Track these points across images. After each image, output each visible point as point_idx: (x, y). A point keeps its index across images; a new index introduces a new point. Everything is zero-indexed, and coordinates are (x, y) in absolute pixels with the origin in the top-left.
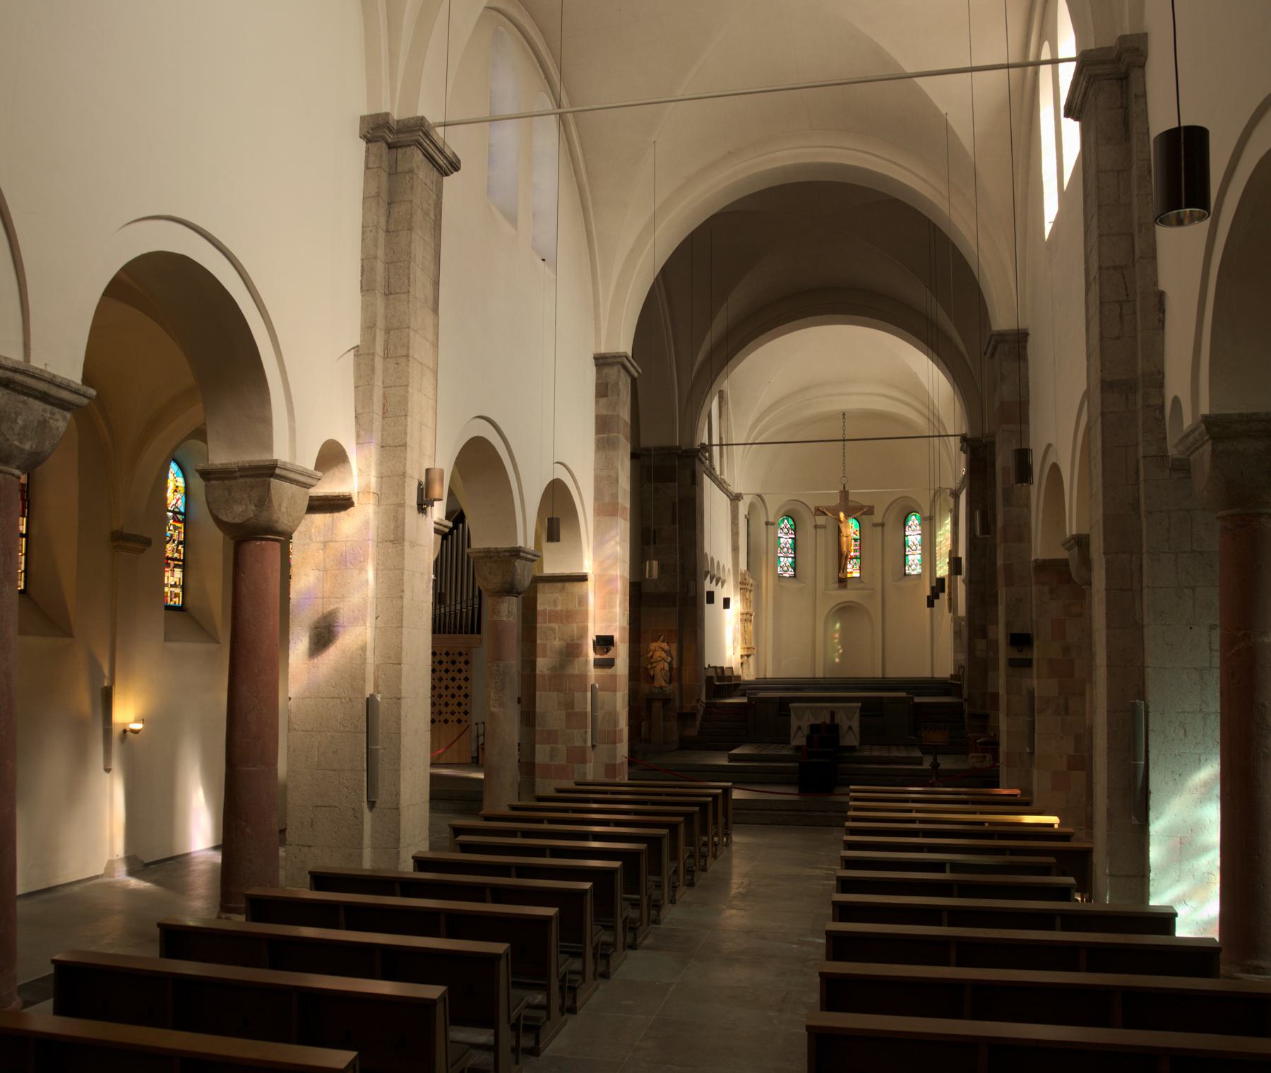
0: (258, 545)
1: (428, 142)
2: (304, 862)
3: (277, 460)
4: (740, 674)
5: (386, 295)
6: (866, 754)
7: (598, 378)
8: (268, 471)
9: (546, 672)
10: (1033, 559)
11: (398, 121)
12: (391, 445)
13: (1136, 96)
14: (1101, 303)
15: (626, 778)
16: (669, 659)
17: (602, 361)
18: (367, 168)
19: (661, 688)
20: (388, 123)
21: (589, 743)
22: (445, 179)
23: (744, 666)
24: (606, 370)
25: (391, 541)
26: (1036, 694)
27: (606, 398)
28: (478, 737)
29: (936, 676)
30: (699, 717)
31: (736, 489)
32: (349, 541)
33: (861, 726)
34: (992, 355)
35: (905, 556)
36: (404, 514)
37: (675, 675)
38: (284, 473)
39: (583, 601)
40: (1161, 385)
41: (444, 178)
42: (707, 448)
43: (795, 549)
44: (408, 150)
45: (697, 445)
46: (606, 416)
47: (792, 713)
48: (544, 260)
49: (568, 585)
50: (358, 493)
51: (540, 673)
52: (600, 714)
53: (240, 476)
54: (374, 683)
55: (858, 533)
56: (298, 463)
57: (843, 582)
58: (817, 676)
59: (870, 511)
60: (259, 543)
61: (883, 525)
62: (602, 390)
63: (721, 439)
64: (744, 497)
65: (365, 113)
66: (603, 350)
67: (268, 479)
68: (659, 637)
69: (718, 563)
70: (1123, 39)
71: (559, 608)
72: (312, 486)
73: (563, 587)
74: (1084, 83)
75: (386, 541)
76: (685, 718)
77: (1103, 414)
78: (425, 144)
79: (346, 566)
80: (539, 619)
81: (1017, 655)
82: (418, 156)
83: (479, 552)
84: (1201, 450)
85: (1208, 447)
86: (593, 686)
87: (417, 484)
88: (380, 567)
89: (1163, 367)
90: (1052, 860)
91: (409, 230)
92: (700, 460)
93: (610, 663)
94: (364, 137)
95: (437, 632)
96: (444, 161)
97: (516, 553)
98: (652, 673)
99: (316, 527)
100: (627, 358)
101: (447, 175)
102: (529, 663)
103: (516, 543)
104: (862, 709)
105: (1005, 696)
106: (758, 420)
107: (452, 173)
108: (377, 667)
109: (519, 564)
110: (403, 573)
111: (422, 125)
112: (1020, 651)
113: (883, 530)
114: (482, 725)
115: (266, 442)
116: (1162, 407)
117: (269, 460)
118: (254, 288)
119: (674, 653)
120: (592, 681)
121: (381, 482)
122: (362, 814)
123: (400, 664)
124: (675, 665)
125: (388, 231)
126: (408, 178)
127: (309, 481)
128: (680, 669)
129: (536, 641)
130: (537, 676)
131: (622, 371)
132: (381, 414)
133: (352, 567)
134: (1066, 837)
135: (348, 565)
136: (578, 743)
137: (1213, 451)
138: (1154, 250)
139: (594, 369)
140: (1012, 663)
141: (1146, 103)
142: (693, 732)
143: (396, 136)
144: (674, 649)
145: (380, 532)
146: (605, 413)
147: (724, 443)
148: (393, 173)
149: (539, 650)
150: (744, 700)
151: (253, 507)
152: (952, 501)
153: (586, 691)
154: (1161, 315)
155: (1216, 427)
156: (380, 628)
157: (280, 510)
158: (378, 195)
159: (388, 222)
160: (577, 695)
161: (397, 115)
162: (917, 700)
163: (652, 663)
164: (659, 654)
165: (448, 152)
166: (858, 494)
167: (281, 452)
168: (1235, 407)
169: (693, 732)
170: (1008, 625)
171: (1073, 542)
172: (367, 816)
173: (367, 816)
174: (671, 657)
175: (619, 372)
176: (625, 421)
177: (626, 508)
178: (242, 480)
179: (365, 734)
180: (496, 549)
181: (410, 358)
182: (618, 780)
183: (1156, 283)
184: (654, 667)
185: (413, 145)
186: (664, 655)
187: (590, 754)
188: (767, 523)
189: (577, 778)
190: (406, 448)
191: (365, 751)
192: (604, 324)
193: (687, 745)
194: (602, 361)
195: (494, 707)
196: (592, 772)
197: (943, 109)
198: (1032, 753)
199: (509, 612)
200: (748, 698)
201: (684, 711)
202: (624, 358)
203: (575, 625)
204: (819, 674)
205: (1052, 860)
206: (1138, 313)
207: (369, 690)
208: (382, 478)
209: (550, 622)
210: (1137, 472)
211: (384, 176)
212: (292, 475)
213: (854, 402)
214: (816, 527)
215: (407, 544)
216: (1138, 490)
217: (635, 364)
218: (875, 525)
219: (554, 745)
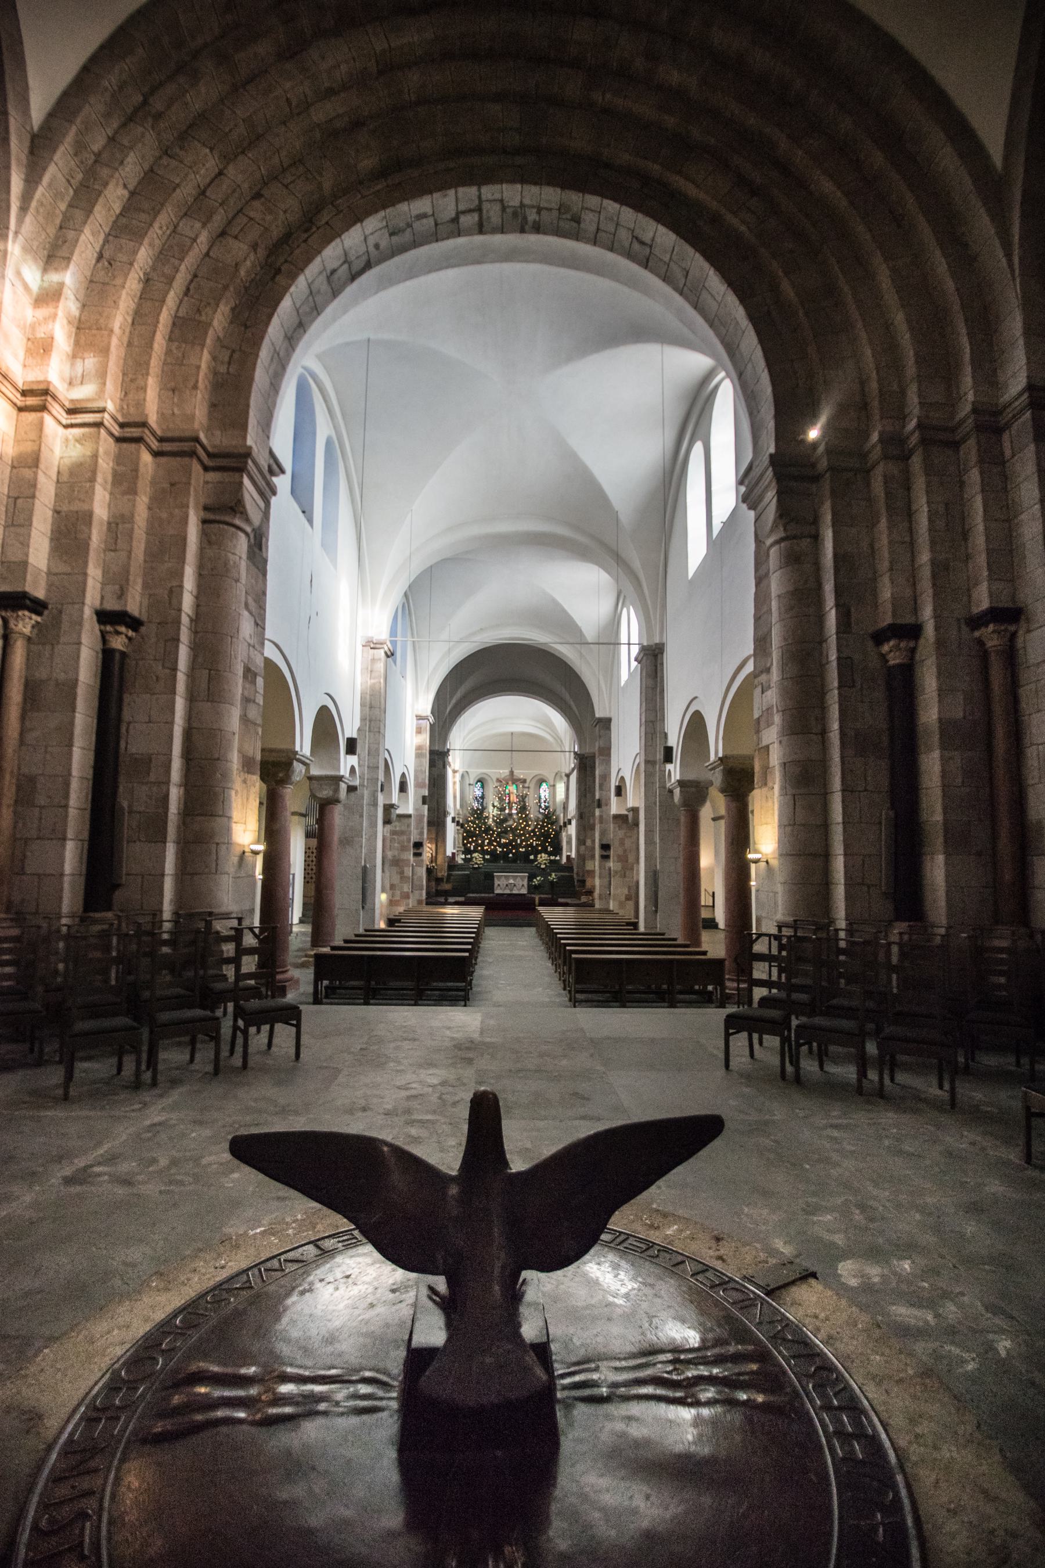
39: (409, 826)
52: (415, 877)
59: (524, 781)
136: (406, 890)
152: (565, 779)
160: (406, 869)
166: (519, 773)
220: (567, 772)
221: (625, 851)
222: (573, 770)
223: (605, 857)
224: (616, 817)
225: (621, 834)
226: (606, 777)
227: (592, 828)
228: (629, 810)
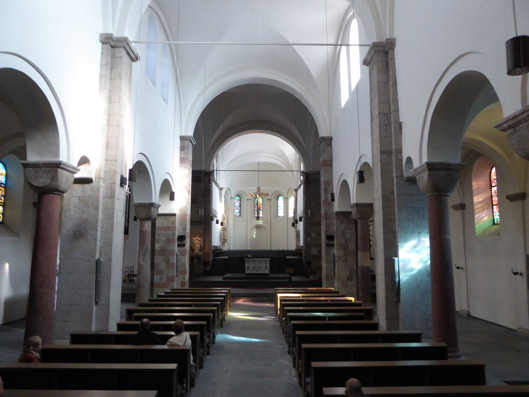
0: (51, 196)
1: (128, 47)
2: (63, 329)
3: (62, 161)
4: (222, 248)
5: (109, 103)
6: (271, 276)
7: (181, 144)
8: (58, 165)
9: (159, 249)
10: (335, 211)
11: (116, 38)
12: (110, 160)
13: (391, 59)
14: (380, 125)
15: (188, 287)
16: (200, 243)
17: (182, 138)
18: (102, 53)
19: (197, 253)
20: (112, 37)
21: (175, 275)
22: (133, 63)
23: (223, 246)
24: (184, 141)
25: (109, 197)
26: (336, 255)
27: (184, 151)
28: (126, 272)
29: (289, 249)
30: (210, 263)
31: (221, 186)
32: (90, 197)
33: (270, 267)
34: (320, 144)
35: (278, 210)
36: (115, 187)
37: (202, 249)
38: (64, 167)
40: (401, 153)
41: (133, 62)
42: (213, 171)
43: (240, 207)
44: (120, 49)
45: (211, 171)
46: (184, 157)
47: (246, 262)
48: (164, 100)
49: (168, 217)
50: (95, 178)
51: (157, 249)
52: (179, 264)
53: (43, 167)
54: (100, 253)
55: (262, 202)
56: (70, 163)
57: (258, 218)
58: (248, 249)
59: (267, 195)
60: (50, 195)
61: (270, 200)
62: (182, 148)
63: (216, 169)
64: (224, 188)
65: (102, 32)
66: (183, 134)
67: (57, 169)
68: (197, 235)
69: (216, 210)
70: (388, 39)
71: (165, 225)
72: (76, 173)
73: (166, 218)
74: (373, 53)
75: (107, 197)
76: (206, 264)
77: (381, 161)
78: (127, 47)
79: (89, 206)
80: (157, 230)
81: (329, 243)
82: (124, 52)
83: (137, 204)
84: (422, 174)
85: (427, 173)
86: (177, 254)
87: (120, 176)
88: (104, 207)
89: (401, 147)
90: (363, 314)
91: (120, 79)
92: (212, 175)
93: (184, 245)
94: (101, 42)
95: (126, 234)
96: (134, 56)
97: (152, 205)
98: (194, 248)
99: (75, 190)
100: (192, 138)
101: (134, 61)
102: (153, 246)
103: (152, 201)
104: (270, 261)
105: (325, 256)
106: (230, 163)
107: (136, 61)
108: (101, 247)
109: (153, 209)
110: (114, 210)
111: (126, 40)
112: (330, 241)
113: (270, 202)
114: (127, 268)
115: (57, 153)
116: (401, 160)
117: (58, 161)
118: (55, 91)
119: (202, 241)
120: (176, 252)
121: (105, 174)
122: (92, 306)
123: (111, 246)
124: (202, 245)
125: (110, 79)
126: (119, 60)
127: (75, 171)
128: (204, 247)
129: (155, 238)
130: (155, 251)
131: (190, 142)
132: (106, 147)
133: (91, 207)
134: (359, 305)
135: (90, 206)
136: (171, 274)
137: (429, 175)
138: (398, 109)
139: (179, 141)
140: (328, 245)
141: (394, 61)
142: (208, 269)
143: (114, 43)
144: (202, 240)
145: (104, 194)
146: (183, 156)
147: (218, 170)
148: (113, 57)
149: (156, 241)
150: (227, 257)
151: (49, 180)
152: (294, 193)
153: (174, 255)
154: (401, 130)
155: (431, 166)
156: (103, 231)
157: (62, 182)
158: (107, 64)
159: (110, 75)
160: (171, 257)
161: (116, 35)
162: (288, 257)
163: (194, 245)
164: (196, 241)
165: (136, 53)
166: (263, 189)
167: (63, 158)
168: (435, 160)
169: (208, 269)
170: (326, 232)
171: (354, 205)
172: (95, 307)
173: (95, 307)
174: (201, 242)
175: (189, 142)
176: (190, 160)
177: (190, 190)
178: (44, 169)
179: (95, 274)
180: (144, 203)
181: (119, 127)
182: (185, 288)
183: (399, 119)
184: (194, 246)
185: (122, 47)
186: (198, 242)
187: (175, 279)
188: (231, 198)
189: (171, 288)
190: (116, 162)
191: (95, 281)
192: (184, 125)
193: (206, 273)
194: (182, 138)
195: (141, 262)
196: (176, 285)
197: (307, 63)
198: (334, 275)
199: (148, 226)
200: (229, 257)
201: (206, 261)
202: (191, 138)
203: (170, 232)
204: (249, 249)
205: (363, 314)
206: (393, 128)
207: (97, 256)
208: (105, 172)
209: (161, 231)
210: (393, 181)
211: (109, 58)
212: (68, 168)
213: (262, 160)
214: (248, 199)
215: (116, 199)
216: (393, 187)
217: (194, 139)
218: (268, 200)
219: (162, 276)
220: (295, 187)
221: (346, 240)
222: (300, 186)
223: (330, 246)
224: (338, 214)
225: (342, 227)
226: (329, 183)
227: (319, 224)
228: (352, 206)
